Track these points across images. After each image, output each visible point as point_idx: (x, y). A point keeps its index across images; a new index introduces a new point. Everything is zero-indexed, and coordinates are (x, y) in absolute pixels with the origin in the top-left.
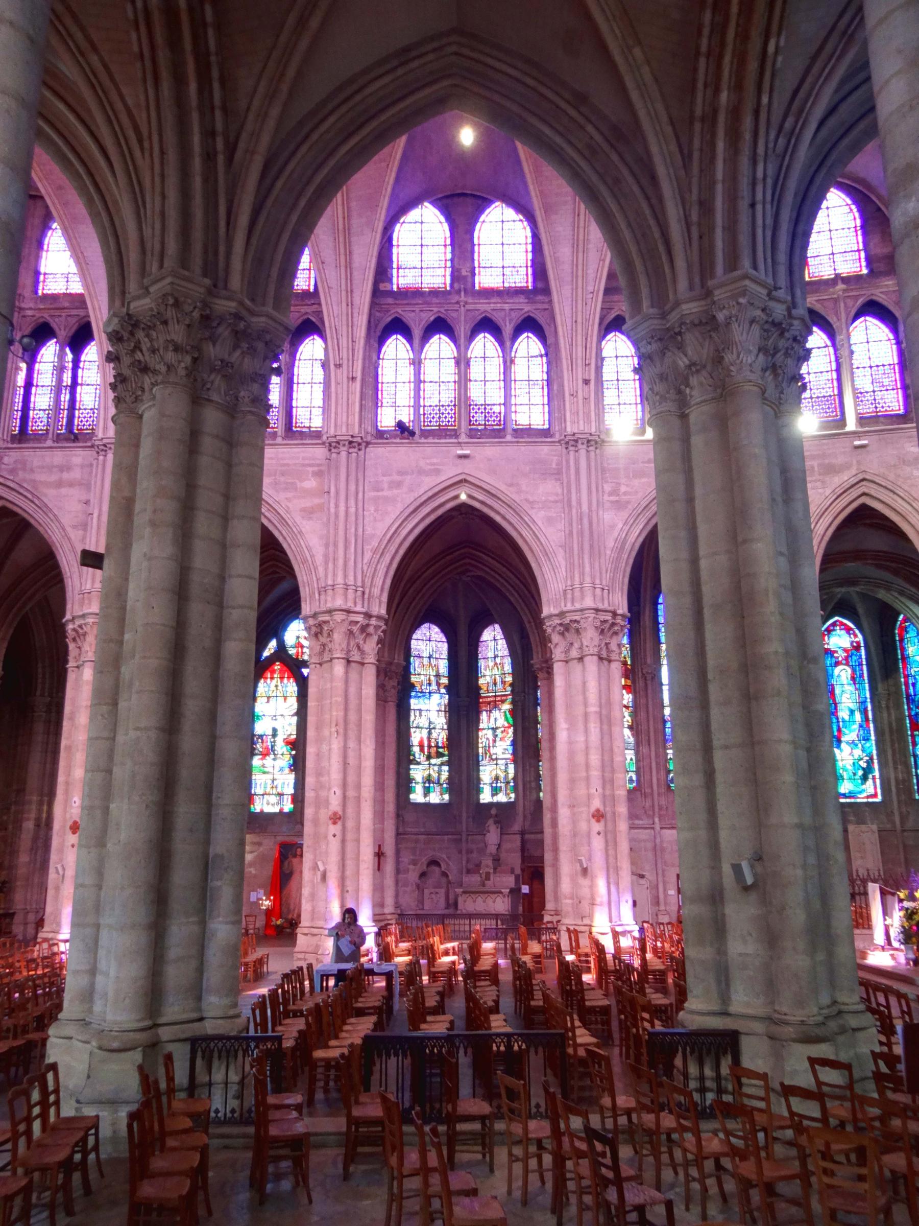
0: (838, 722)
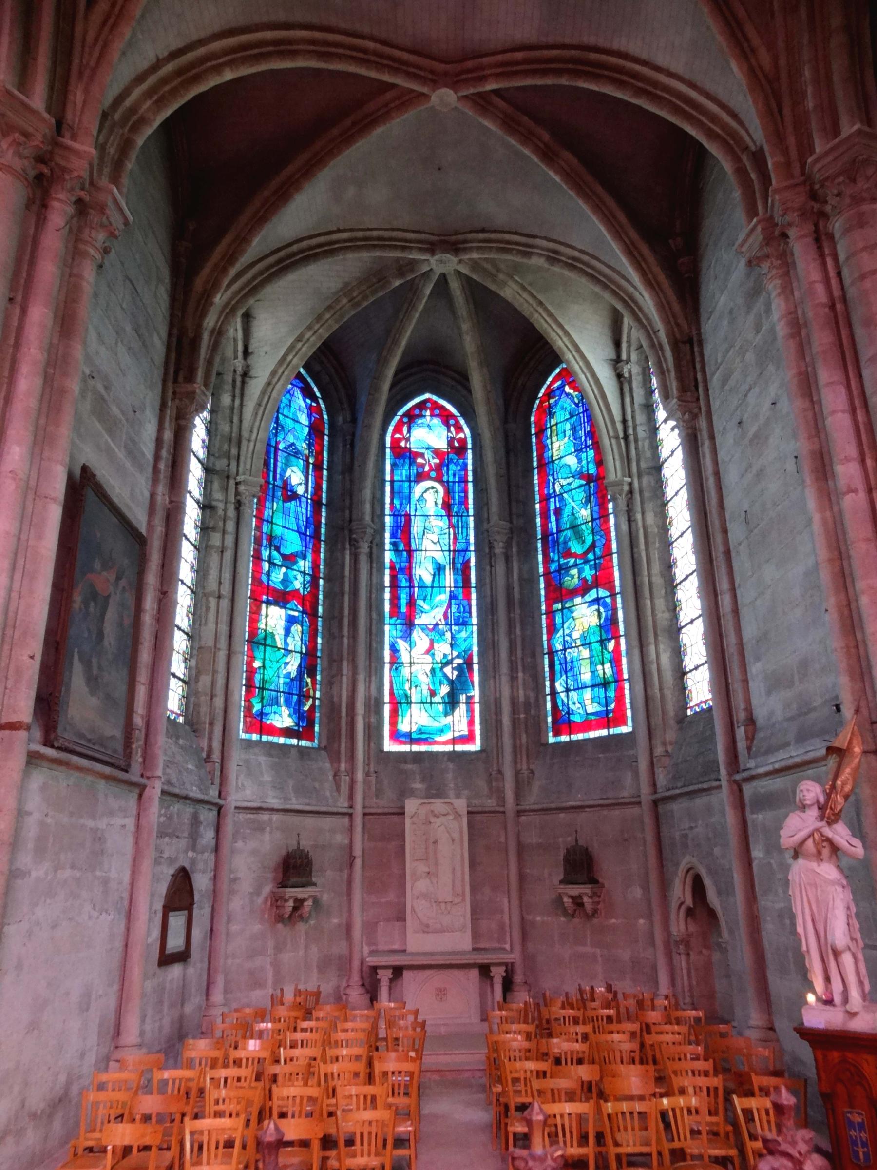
0: (411, 587)
